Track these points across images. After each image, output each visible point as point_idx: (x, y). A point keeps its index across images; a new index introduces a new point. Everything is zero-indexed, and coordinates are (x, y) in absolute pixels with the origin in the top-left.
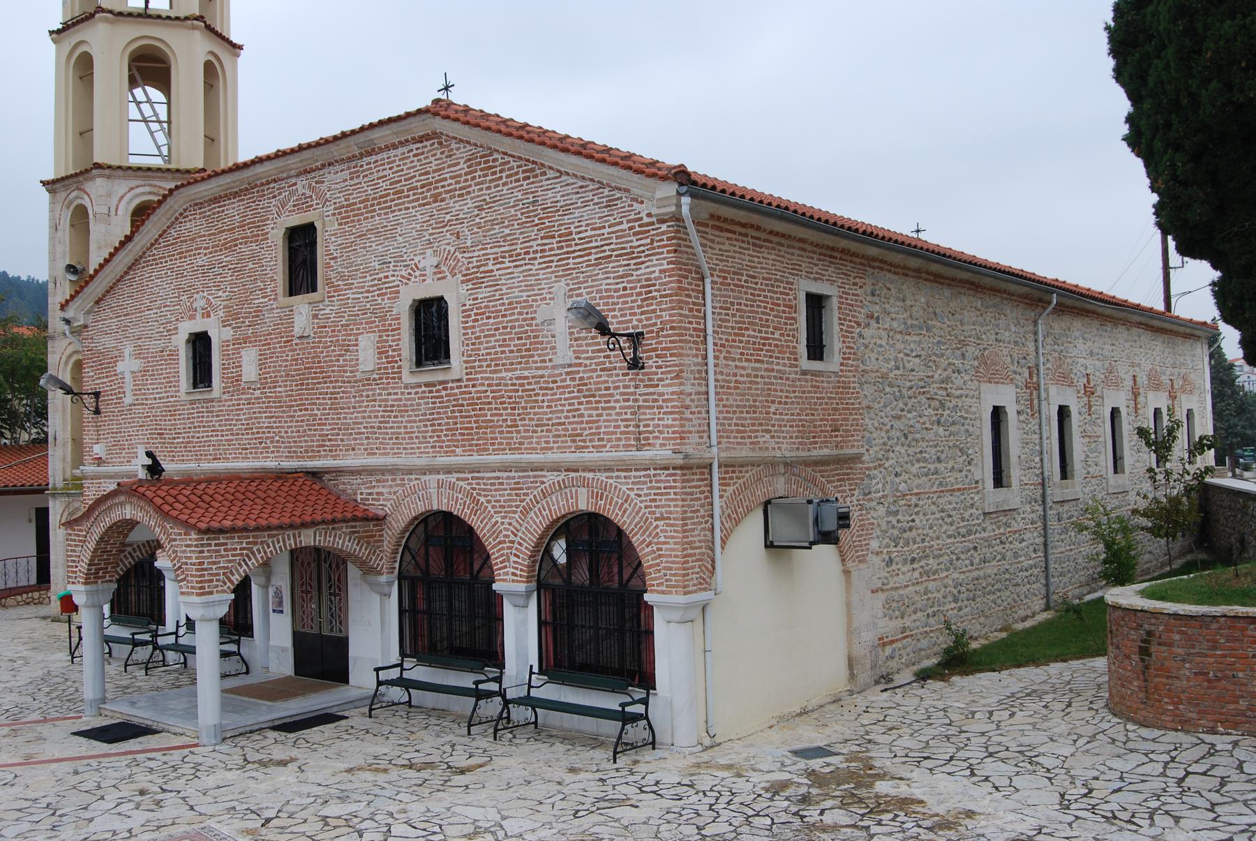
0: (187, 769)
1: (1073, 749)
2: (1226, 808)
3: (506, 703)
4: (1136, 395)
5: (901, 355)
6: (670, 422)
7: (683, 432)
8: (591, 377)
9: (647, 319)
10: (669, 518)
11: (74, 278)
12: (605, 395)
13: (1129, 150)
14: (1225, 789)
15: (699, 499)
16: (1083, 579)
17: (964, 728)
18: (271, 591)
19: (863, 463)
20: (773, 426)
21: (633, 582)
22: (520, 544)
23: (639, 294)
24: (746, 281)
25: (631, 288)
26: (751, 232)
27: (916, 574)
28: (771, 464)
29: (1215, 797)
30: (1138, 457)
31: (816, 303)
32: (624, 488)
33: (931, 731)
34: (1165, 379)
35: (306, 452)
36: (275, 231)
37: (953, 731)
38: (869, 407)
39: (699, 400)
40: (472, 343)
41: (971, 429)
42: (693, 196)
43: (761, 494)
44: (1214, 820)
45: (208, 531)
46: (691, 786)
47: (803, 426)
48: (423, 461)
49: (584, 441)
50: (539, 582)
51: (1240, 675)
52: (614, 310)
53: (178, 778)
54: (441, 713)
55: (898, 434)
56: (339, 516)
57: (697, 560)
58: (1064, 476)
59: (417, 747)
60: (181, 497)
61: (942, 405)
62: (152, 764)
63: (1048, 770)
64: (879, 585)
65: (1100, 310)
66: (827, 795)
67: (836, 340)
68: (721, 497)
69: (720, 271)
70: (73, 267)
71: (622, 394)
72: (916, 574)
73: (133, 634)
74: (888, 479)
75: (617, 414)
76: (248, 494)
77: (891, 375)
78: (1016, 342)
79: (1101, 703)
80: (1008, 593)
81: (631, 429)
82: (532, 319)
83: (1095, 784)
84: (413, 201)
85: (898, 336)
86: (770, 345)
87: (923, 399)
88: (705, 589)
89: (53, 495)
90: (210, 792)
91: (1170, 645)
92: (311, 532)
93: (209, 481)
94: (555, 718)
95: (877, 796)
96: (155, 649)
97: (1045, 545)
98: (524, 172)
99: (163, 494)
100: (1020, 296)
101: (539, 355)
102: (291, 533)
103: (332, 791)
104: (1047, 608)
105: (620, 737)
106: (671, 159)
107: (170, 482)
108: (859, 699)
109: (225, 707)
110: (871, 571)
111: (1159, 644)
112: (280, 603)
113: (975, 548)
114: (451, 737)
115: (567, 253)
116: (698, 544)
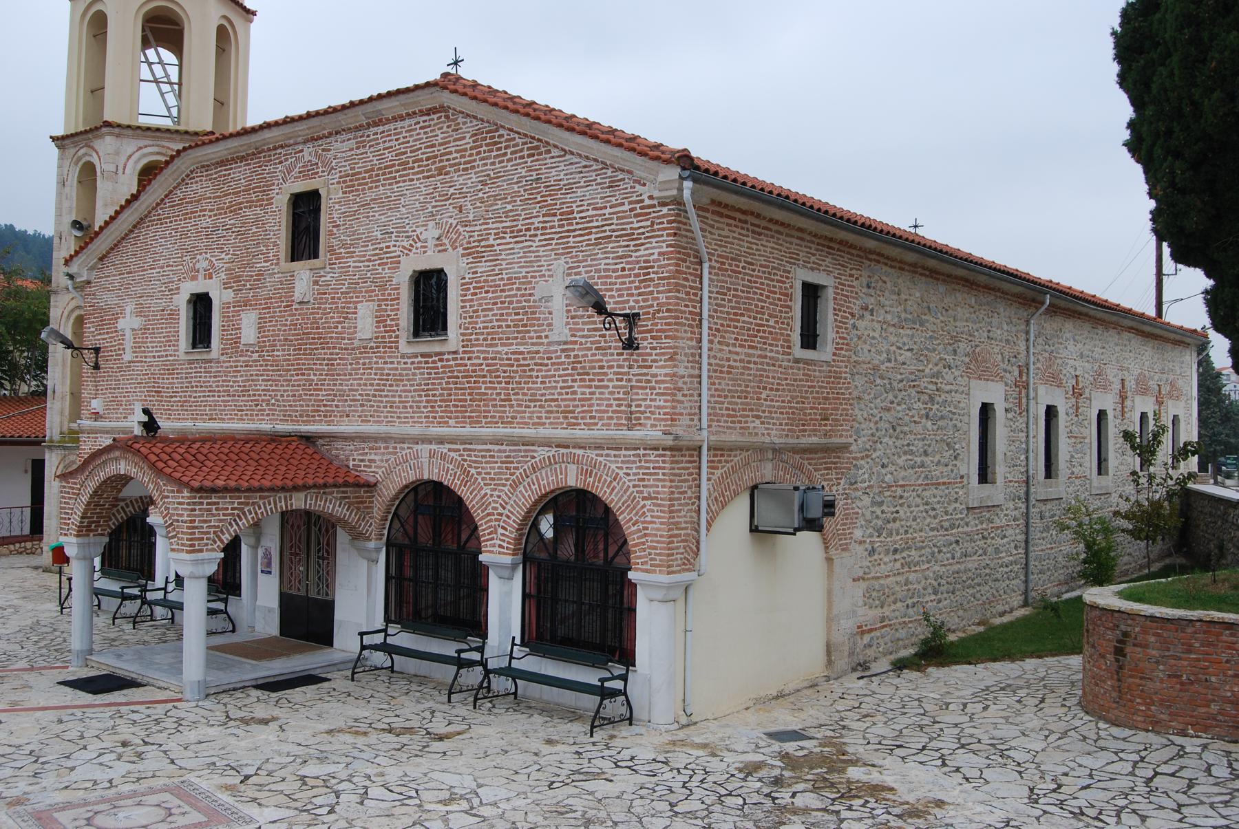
0: (169, 723)
1: (1044, 745)
2: (1193, 810)
3: (488, 672)
4: (1123, 398)
5: (894, 348)
6: (662, 403)
7: (675, 414)
8: (586, 355)
9: (644, 301)
10: (656, 498)
11: (79, 234)
12: (598, 374)
13: (1129, 155)
14: (1193, 791)
15: (687, 481)
16: (1062, 578)
17: (937, 719)
18: (260, 552)
19: (850, 452)
20: (764, 412)
21: (617, 560)
22: (508, 517)
23: (637, 275)
24: (744, 268)
25: (630, 269)
26: (750, 219)
27: (898, 565)
28: (760, 451)
29: (1182, 799)
30: (1122, 460)
31: (811, 293)
32: (613, 466)
33: (904, 721)
34: (1153, 384)
35: (301, 416)
36: (280, 196)
37: (927, 721)
38: (859, 398)
39: (692, 383)
40: (470, 316)
41: (959, 425)
42: (695, 181)
43: (748, 479)
44: (1180, 821)
45: (200, 490)
46: (666, 763)
47: (793, 413)
48: (416, 431)
49: (576, 418)
50: (525, 554)
51: (1213, 679)
52: (612, 290)
53: (161, 732)
54: (423, 680)
55: (887, 426)
56: (331, 481)
57: (682, 541)
58: (1048, 475)
59: (397, 712)
60: (175, 455)
61: (932, 399)
62: (135, 717)
63: (1019, 764)
64: (861, 574)
65: (1092, 313)
66: (799, 778)
67: (830, 329)
68: (709, 479)
69: (719, 256)
70: (78, 223)
71: (616, 373)
72: (898, 565)
73: (123, 588)
74: (875, 470)
75: (610, 393)
76: (242, 455)
77: (883, 367)
78: (1007, 341)
79: (1075, 701)
80: (987, 588)
81: (623, 408)
82: (530, 295)
83: (1064, 780)
84: (418, 173)
85: (892, 329)
86: (764, 332)
87: (913, 392)
88: (688, 570)
89: (50, 447)
90: (192, 747)
91: (1146, 646)
92: (302, 495)
93: (204, 440)
94: (535, 690)
95: (849, 782)
96: (143, 603)
97: (1027, 542)
98: (529, 149)
99: (157, 451)
100: (1014, 295)
101: (535, 331)
102: (282, 495)
103: (312, 752)
104: (1025, 604)
105: (598, 712)
106: (675, 143)
107: (166, 440)
108: (835, 685)
109: (210, 664)
110: (853, 559)
111: (1135, 645)
112: (269, 564)
113: (957, 542)
114: (431, 704)
115: (568, 231)
116: (683, 525)
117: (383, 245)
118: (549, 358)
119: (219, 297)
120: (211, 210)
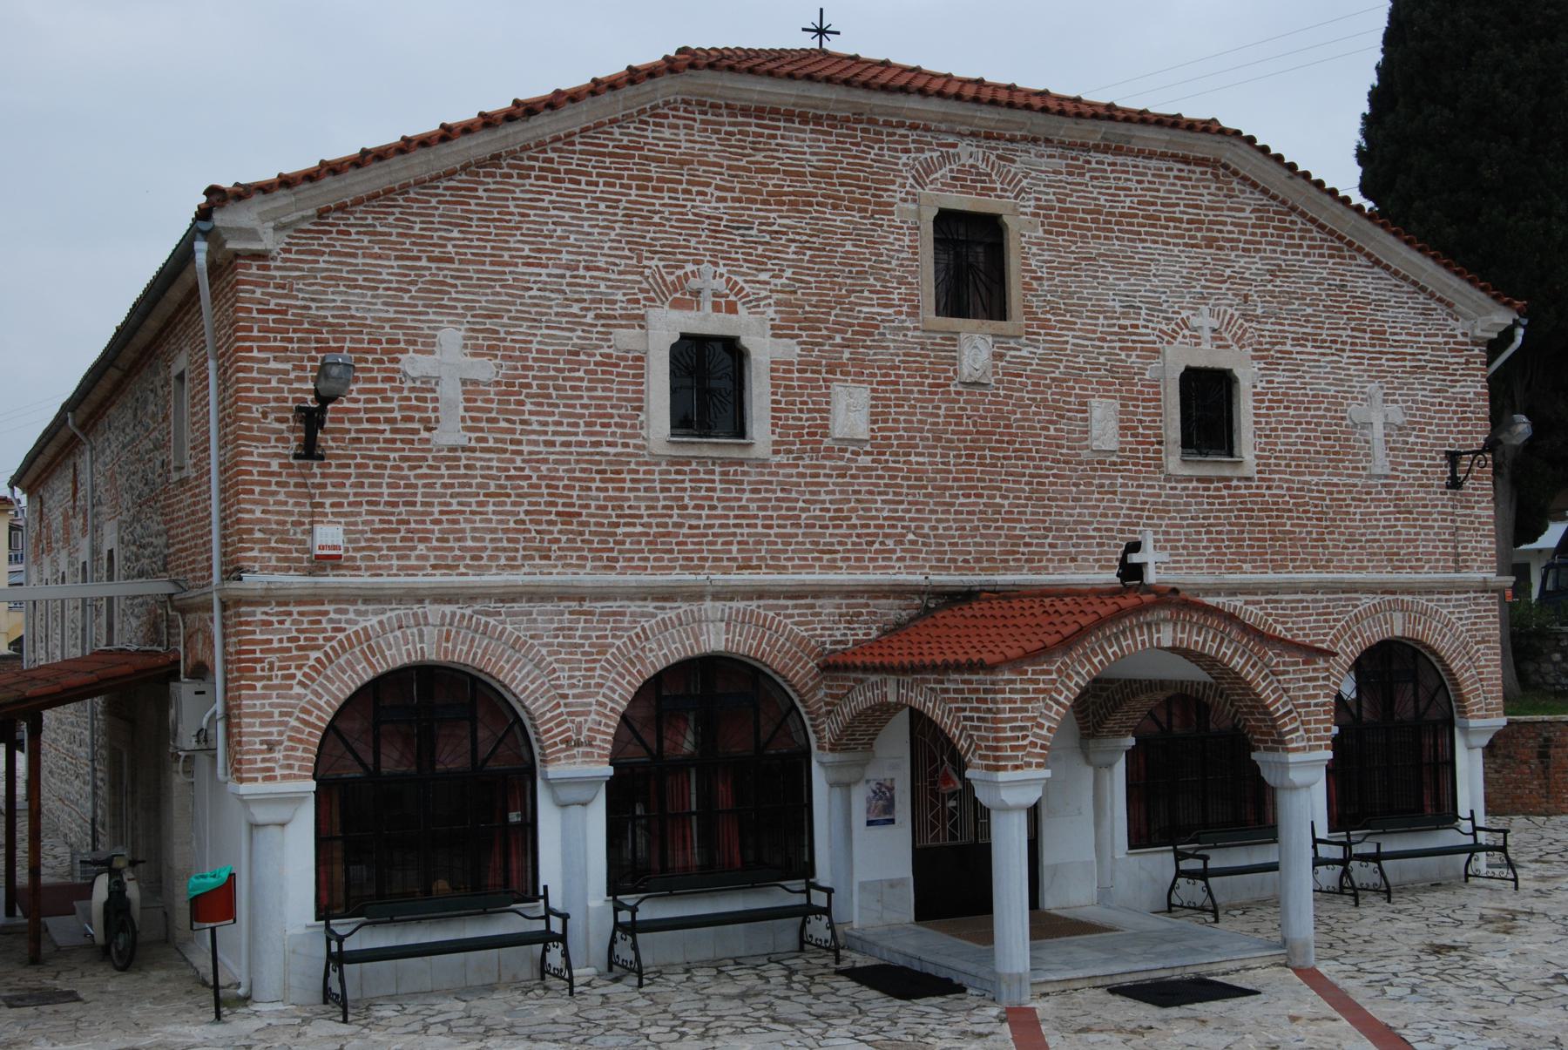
23: (1455, 412)
35: (978, 560)
40: (1266, 435)
82: (1343, 418)
84: (1176, 236)
98: (1330, 248)
101: (1351, 461)
107: (1150, 589)
112: (889, 806)
117: (1127, 322)
118: (1368, 493)
120: (718, 188)
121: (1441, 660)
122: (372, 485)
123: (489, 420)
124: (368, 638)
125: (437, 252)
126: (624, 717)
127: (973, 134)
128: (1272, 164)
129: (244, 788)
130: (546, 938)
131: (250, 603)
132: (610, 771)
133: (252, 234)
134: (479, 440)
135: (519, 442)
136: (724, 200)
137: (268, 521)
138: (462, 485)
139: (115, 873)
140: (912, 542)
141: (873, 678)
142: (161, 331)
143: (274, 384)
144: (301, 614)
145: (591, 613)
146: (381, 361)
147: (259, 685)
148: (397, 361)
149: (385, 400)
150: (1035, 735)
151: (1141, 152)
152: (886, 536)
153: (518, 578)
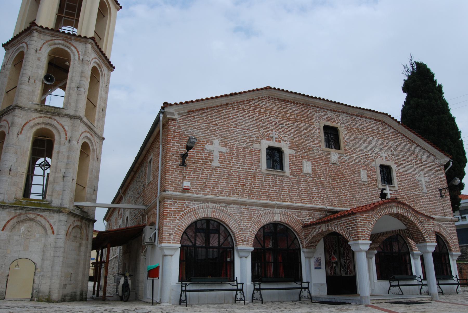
35: (338, 204)
40: (400, 181)
112: (320, 264)
119: (287, 152)
121: (444, 237)
122: (197, 174)
123: (225, 161)
124: (195, 210)
125: (214, 123)
126: (256, 237)
127: (330, 110)
128: (394, 122)
129: (163, 245)
130: (237, 290)
131: (167, 199)
132: (253, 249)
133: (173, 114)
134: (222, 165)
135: (232, 167)
136: (276, 118)
137: (173, 180)
138: (218, 176)
139: (125, 277)
140: (323, 199)
141: (318, 226)
142: (146, 154)
143: (176, 148)
144: (179, 202)
145: (248, 209)
146: (200, 146)
147: (168, 219)
148: (204, 146)
149: (201, 154)
150: (367, 232)
151: (366, 117)
152: (317, 197)
153: (231, 198)
